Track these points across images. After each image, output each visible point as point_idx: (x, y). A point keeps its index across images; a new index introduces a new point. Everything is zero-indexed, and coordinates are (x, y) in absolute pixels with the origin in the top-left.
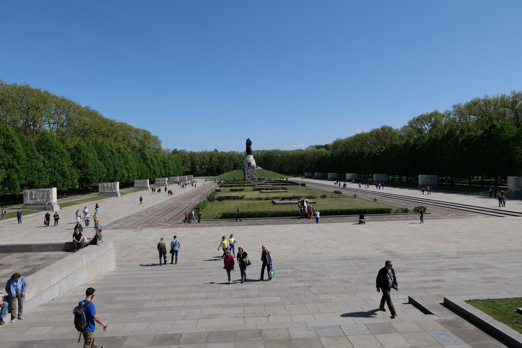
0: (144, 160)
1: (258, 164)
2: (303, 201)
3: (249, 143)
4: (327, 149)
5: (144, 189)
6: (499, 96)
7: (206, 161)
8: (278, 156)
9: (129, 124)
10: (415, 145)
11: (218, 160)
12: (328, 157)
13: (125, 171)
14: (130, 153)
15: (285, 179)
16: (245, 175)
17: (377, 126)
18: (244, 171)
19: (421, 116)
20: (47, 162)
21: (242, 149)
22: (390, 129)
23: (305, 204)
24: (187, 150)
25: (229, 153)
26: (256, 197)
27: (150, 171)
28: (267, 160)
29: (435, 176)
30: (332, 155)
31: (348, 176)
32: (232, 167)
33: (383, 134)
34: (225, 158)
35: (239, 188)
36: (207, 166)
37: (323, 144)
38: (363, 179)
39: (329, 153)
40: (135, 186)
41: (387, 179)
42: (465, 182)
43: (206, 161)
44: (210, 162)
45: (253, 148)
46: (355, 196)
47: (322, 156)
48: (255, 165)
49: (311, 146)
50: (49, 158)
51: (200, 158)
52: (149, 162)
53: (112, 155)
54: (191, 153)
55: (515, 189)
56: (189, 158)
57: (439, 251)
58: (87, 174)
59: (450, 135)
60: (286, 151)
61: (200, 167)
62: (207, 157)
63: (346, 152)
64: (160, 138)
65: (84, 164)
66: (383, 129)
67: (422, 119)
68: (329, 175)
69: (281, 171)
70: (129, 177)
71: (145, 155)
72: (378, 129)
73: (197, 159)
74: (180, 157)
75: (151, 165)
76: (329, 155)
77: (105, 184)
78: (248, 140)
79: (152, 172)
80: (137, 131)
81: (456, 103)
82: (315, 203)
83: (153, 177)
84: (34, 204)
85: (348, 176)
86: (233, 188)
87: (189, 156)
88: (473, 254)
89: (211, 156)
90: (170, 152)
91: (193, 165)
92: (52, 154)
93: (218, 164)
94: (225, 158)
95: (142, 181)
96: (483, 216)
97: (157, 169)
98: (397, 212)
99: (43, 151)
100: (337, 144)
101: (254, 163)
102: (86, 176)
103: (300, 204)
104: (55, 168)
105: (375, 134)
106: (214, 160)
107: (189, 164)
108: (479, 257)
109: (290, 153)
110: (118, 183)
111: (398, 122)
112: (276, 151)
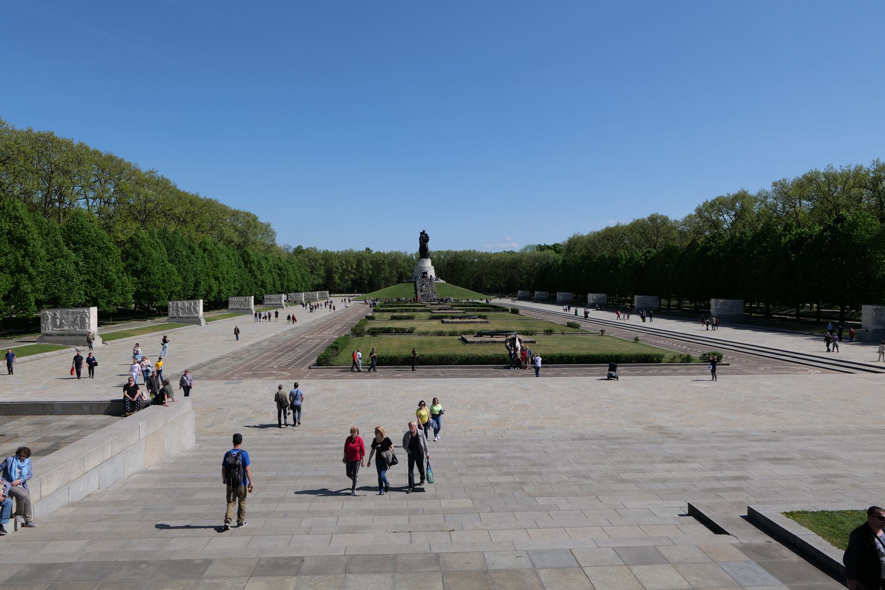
0: (246, 263)
1: (439, 274)
2: (514, 339)
3: (424, 239)
4: (557, 252)
5: (246, 313)
6: (852, 168)
7: (352, 267)
8: (472, 262)
9: (222, 201)
10: (705, 249)
11: (371, 267)
12: (558, 265)
13: (213, 281)
14: (222, 251)
15: (484, 301)
16: (416, 293)
17: (644, 214)
18: (415, 286)
19: (717, 199)
20: (81, 264)
21: (413, 249)
22: (665, 220)
23: (518, 343)
24: (318, 249)
25: (391, 254)
26: (433, 330)
27: (256, 283)
28: (455, 268)
29: (739, 302)
30: (564, 261)
31: (592, 297)
32: (396, 279)
33: (652, 229)
34: (383, 263)
35: (405, 314)
37: (550, 243)
38: (616, 303)
40: (230, 307)
41: (656, 305)
42: (789, 314)
43: (352, 267)
44: (357, 269)
45: (432, 247)
46: (603, 331)
47: (548, 263)
48: (434, 276)
49: (529, 246)
50: (86, 256)
52: (254, 267)
53: (193, 253)
54: (326, 253)
55: (875, 327)
56: (322, 262)
57: (741, 429)
58: (148, 286)
59: (767, 232)
60: (487, 253)
61: (341, 278)
62: (352, 260)
64: (273, 227)
65: (144, 269)
66: (653, 219)
67: (718, 205)
68: (560, 296)
69: (477, 287)
70: (220, 292)
71: (249, 256)
72: (643, 220)
73: (336, 263)
74: (306, 259)
75: (258, 273)
77: (180, 303)
78: (423, 233)
80: (235, 214)
81: (778, 178)
82: (534, 342)
84: (58, 335)
85: (592, 297)
86: (395, 314)
88: (800, 435)
90: (291, 251)
92: (90, 250)
93: (371, 272)
94: (383, 263)
95: (242, 299)
96: (818, 371)
97: (268, 280)
98: (672, 361)
99: (75, 244)
100: (574, 243)
101: (431, 272)
102: (146, 289)
103: (508, 344)
104: (95, 274)
107: (322, 272)
108: (809, 440)
109: (493, 258)
110: (201, 301)
111: (678, 207)
112: (469, 253)
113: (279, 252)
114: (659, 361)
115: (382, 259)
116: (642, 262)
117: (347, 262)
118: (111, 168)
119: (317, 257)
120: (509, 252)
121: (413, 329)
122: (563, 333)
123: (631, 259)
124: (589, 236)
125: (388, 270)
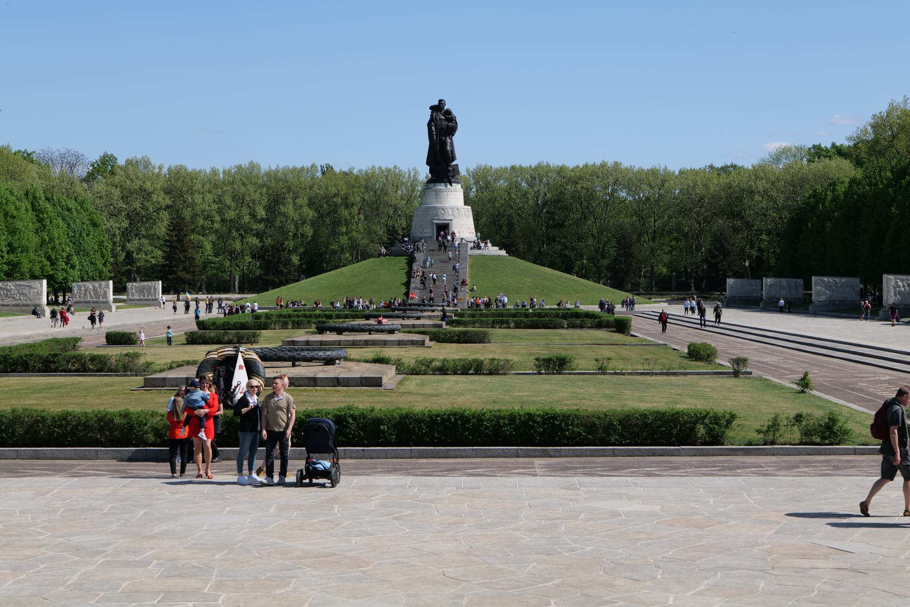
2: (230, 361)
3: (442, 125)
4: (859, 163)
7: (253, 216)
11: (310, 213)
12: (835, 198)
16: (407, 284)
23: (240, 376)
24: (155, 161)
36: (253, 241)
43: (253, 216)
46: (739, 362)
49: (785, 152)
51: (219, 200)
54: (178, 174)
60: (654, 172)
68: (822, 287)
73: (204, 202)
74: (117, 193)
87: (168, 192)
89: (279, 190)
90: (82, 171)
91: (178, 227)
93: (309, 231)
94: (348, 206)
101: (464, 227)
107: (162, 229)
112: (601, 173)
114: (715, 439)
119: (148, 186)
120: (725, 169)
122: (602, 371)
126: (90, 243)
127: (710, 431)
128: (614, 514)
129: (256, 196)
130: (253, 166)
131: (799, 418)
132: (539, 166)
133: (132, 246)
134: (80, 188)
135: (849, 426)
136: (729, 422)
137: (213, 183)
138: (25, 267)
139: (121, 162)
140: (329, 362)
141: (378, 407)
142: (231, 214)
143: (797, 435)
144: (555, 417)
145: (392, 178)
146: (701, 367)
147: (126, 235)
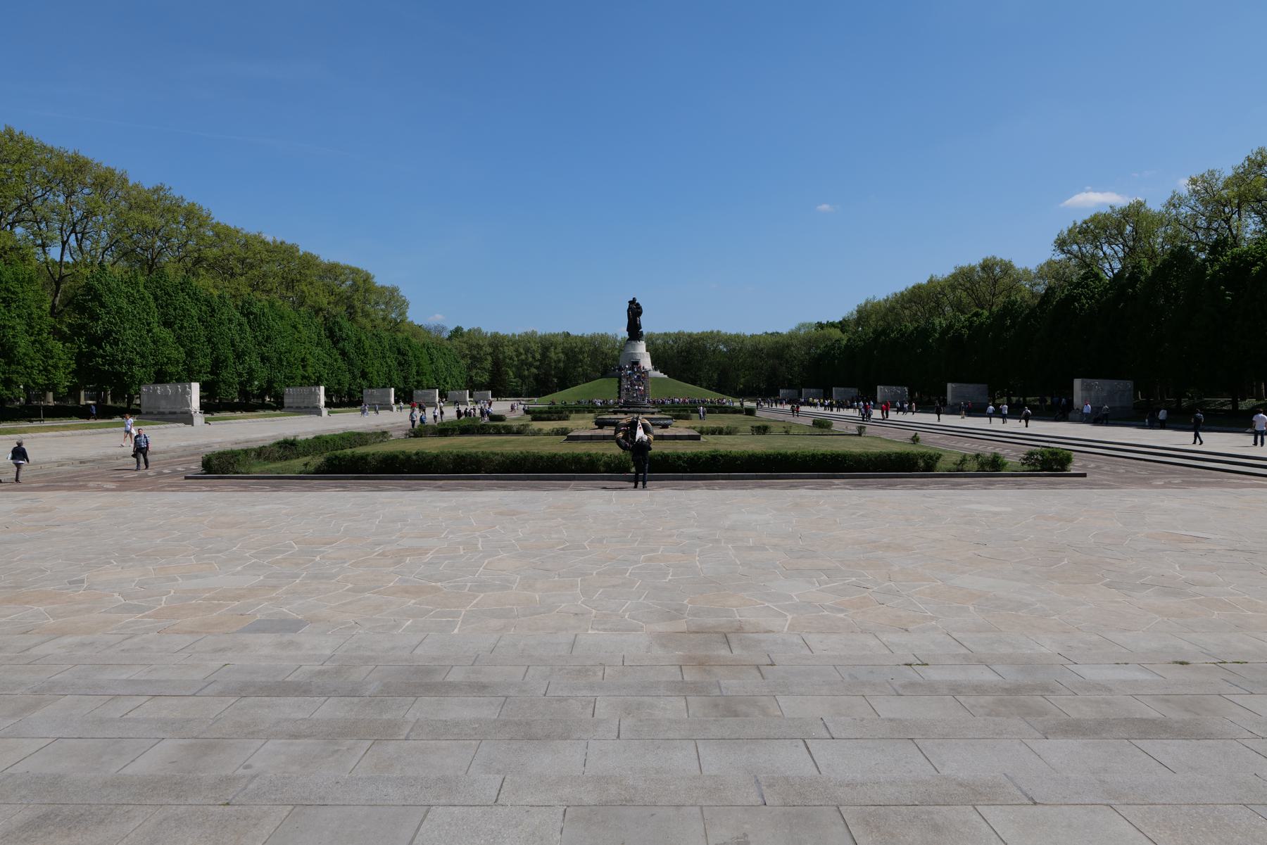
0: (335, 343)
1: (656, 363)
2: (633, 425)
3: (635, 311)
4: (843, 331)
5: (310, 413)
7: (533, 357)
10: (1071, 299)
11: (562, 356)
17: (973, 259)
18: (620, 382)
19: (1092, 220)
22: (1007, 268)
23: (640, 433)
24: (484, 330)
25: (593, 338)
28: (687, 359)
29: (1129, 384)
30: (849, 340)
31: (882, 391)
34: (581, 352)
36: (534, 371)
37: (837, 318)
39: (845, 338)
42: (1222, 402)
43: (533, 357)
49: (803, 325)
51: (517, 350)
52: (349, 347)
56: (489, 350)
57: (1047, 646)
60: (738, 336)
61: (519, 375)
63: (884, 332)
64: (405, 292)
66: (987, 266)
69: (722, 386)
71: (340, 330)
72: (972, 269)
73: (509, 351)
74: (465, 346)
76: (844, 342)
77: (159, 389)
78: (633, 302)
79: (357, 373)
80: (333, 271)
83: (361, 387)
85: (882, 391)
87: (491, 345)
89: (547, 344)
90: (446, 335)
91: (497, 364)
93: (562, 365)
94: (581, 352)
95: (305, 390)
97: (375, 368)
100: (863, 315)
101: (646, 363)
105: (964, 279)
106: (552, 355)
107: (488, 364)
110: (196, 387)
111: (1029, 248)
113: (417, 330)
115: (580, 345)
116: (965, 332)
117: (527, 350)
118: (71, 172)
119: (481, 343)
121: (526, 426)
122: (787, 433)
123: (950, 326)
124: (886, 301)
125: (587, 360)
126: (455, 372)
127: (927, 464)
128: (996, 514)
129: (535, 348)
130: (534, 333)
131: (978, 456)
132: (679, 334)
133: (473, 373)
134: (445, 343)
135: (1006, 460)
136: (938, 458)
137: (514, 341)
138: (425, 383)
139: (466, 330)
140: (665, 426)
141: (689, 451)
142: (523, 357)
143: (976, 467)
144: (838, 455)
145: (604, 339)
146: (818, 431)
147: (469, 368)
